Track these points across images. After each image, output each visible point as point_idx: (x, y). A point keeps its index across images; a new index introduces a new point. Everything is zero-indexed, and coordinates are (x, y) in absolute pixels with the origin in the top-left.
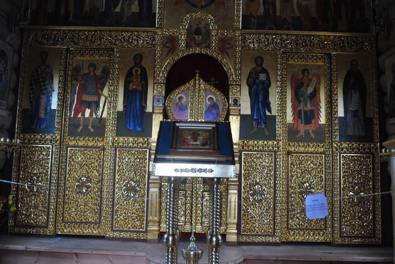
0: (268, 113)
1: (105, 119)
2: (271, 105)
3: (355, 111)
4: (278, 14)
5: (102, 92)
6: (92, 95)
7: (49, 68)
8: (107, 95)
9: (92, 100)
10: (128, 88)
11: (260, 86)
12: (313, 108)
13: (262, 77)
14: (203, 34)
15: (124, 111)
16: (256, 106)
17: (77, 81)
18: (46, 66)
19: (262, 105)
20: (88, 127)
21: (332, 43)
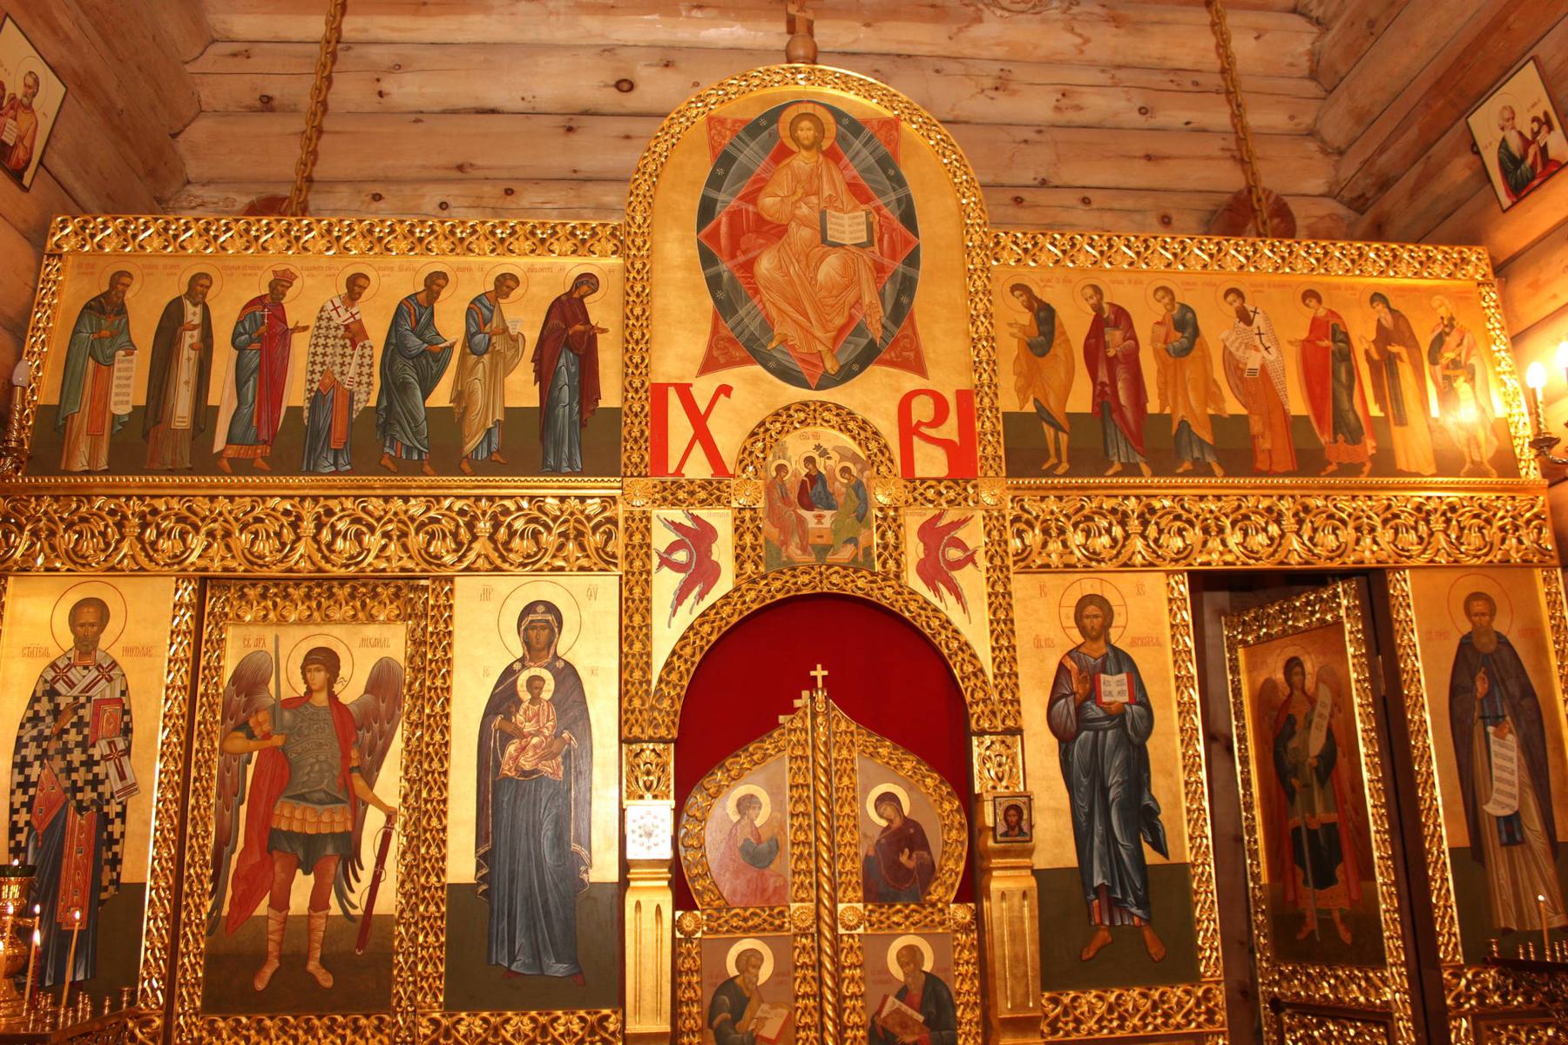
0: (1151, 857)
1: (387, 918)
2: (1160, 817)
3: (1507, 819)
4: (1153, 407)
5: (371, 785)
6: (320, 802)
7: (110, 680)
8: (394, 801)
9: (325, 830)
10: (498, 765)
11: (1105, 730)
12: (1333, 817)
13: (1114, 688)
14: (841, 500)
15: (482, 879)
16: (1098, 828)
17: (251, 736)
18: (99, 667)
19: (1125, 823)
20: (305, 964)
21: (1385, 522)
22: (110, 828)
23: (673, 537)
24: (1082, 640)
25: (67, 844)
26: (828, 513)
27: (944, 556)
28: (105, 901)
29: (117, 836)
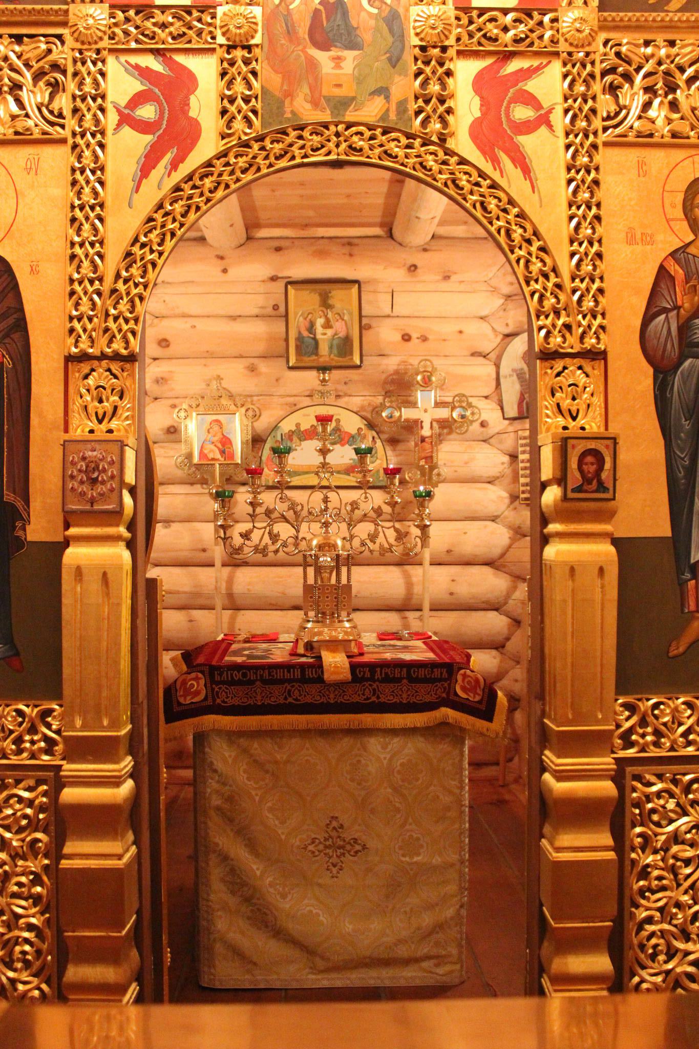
23: (136, 86)
24: (691, 237)
26: (350, 56)
27: (508, 115)
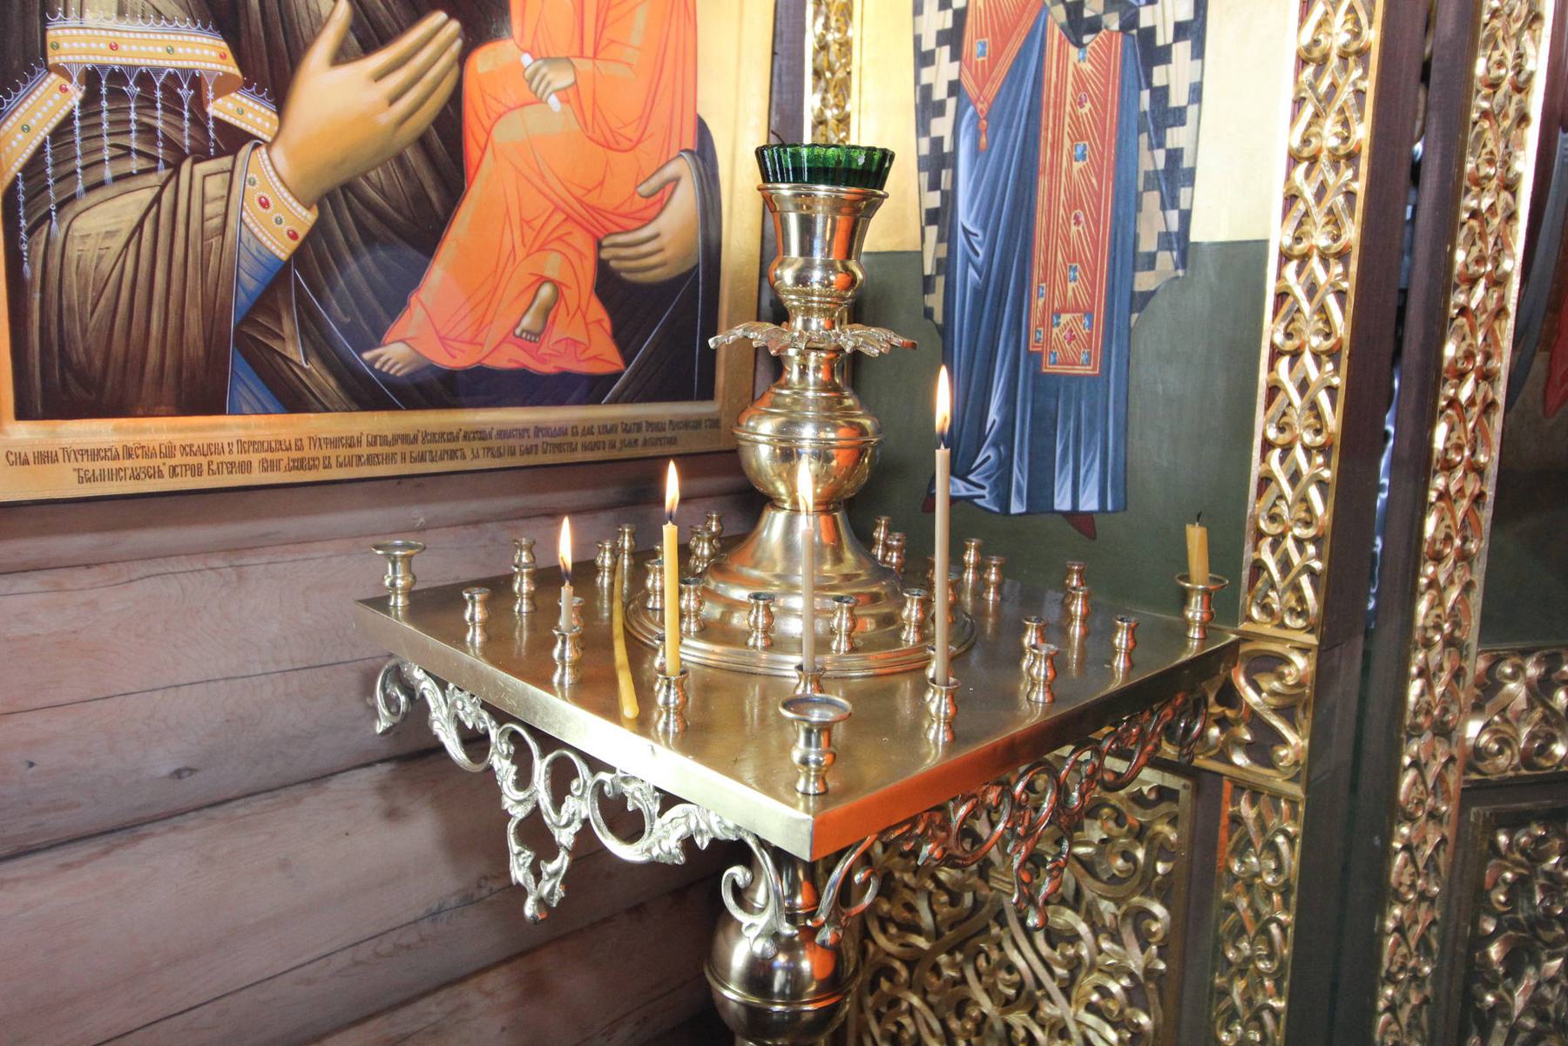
22: (1159, 75)
25: (1047, 136)
28: (1148, 296)
29: (1178, 98)
